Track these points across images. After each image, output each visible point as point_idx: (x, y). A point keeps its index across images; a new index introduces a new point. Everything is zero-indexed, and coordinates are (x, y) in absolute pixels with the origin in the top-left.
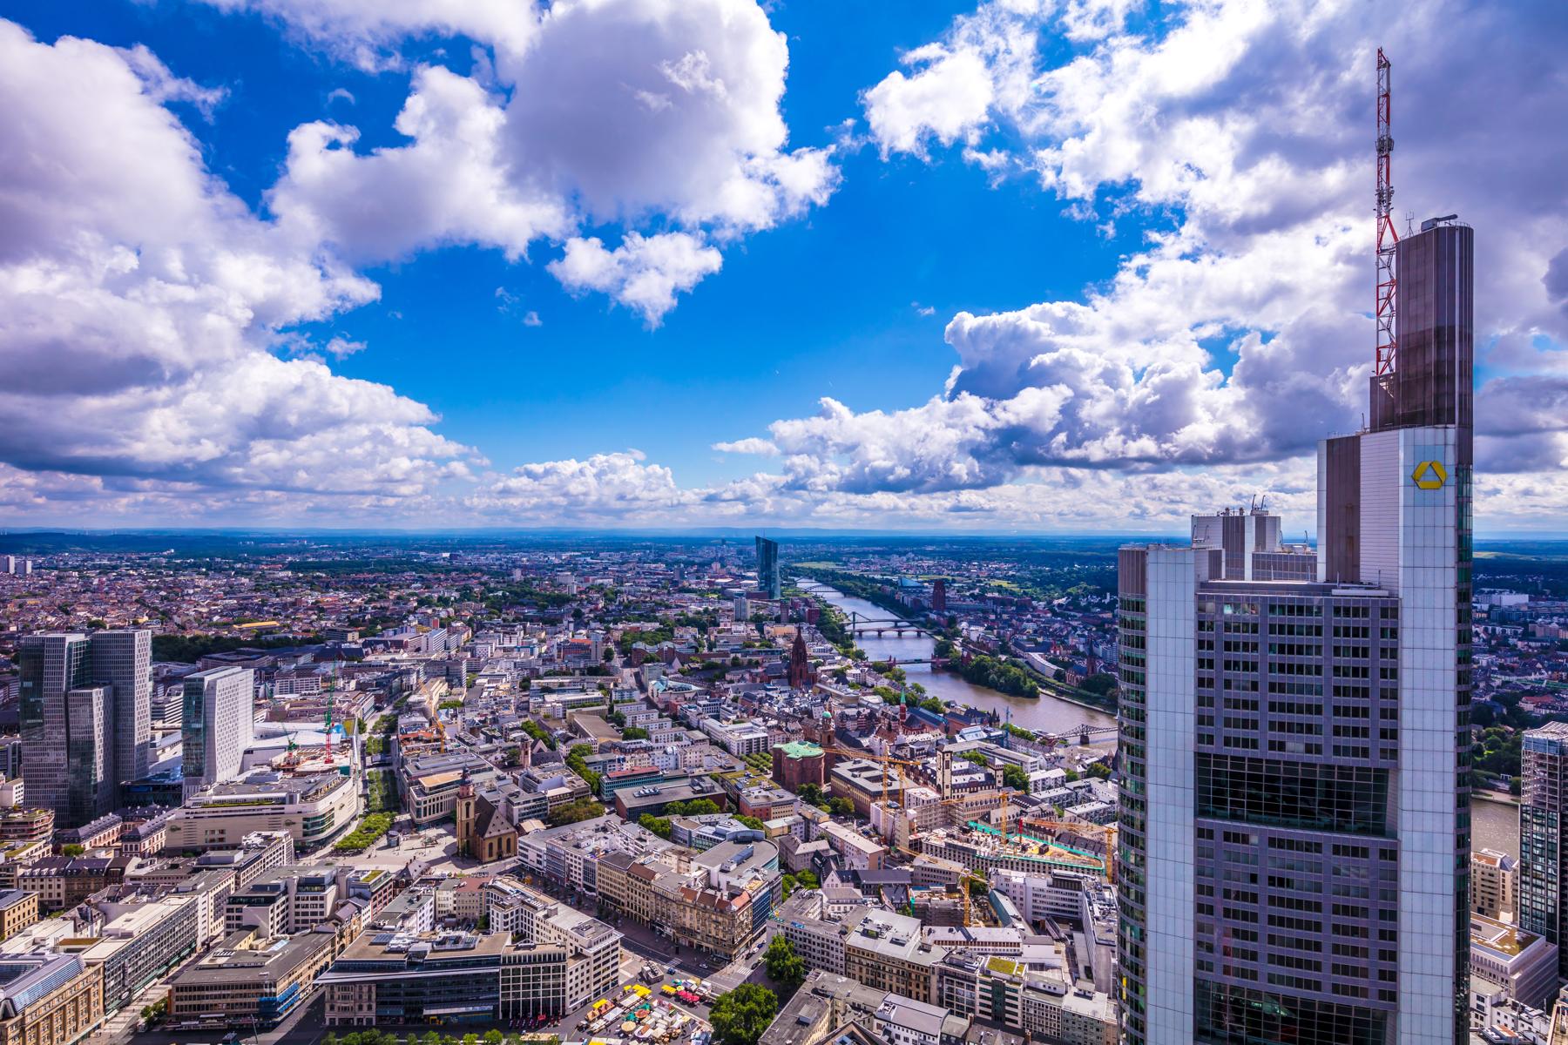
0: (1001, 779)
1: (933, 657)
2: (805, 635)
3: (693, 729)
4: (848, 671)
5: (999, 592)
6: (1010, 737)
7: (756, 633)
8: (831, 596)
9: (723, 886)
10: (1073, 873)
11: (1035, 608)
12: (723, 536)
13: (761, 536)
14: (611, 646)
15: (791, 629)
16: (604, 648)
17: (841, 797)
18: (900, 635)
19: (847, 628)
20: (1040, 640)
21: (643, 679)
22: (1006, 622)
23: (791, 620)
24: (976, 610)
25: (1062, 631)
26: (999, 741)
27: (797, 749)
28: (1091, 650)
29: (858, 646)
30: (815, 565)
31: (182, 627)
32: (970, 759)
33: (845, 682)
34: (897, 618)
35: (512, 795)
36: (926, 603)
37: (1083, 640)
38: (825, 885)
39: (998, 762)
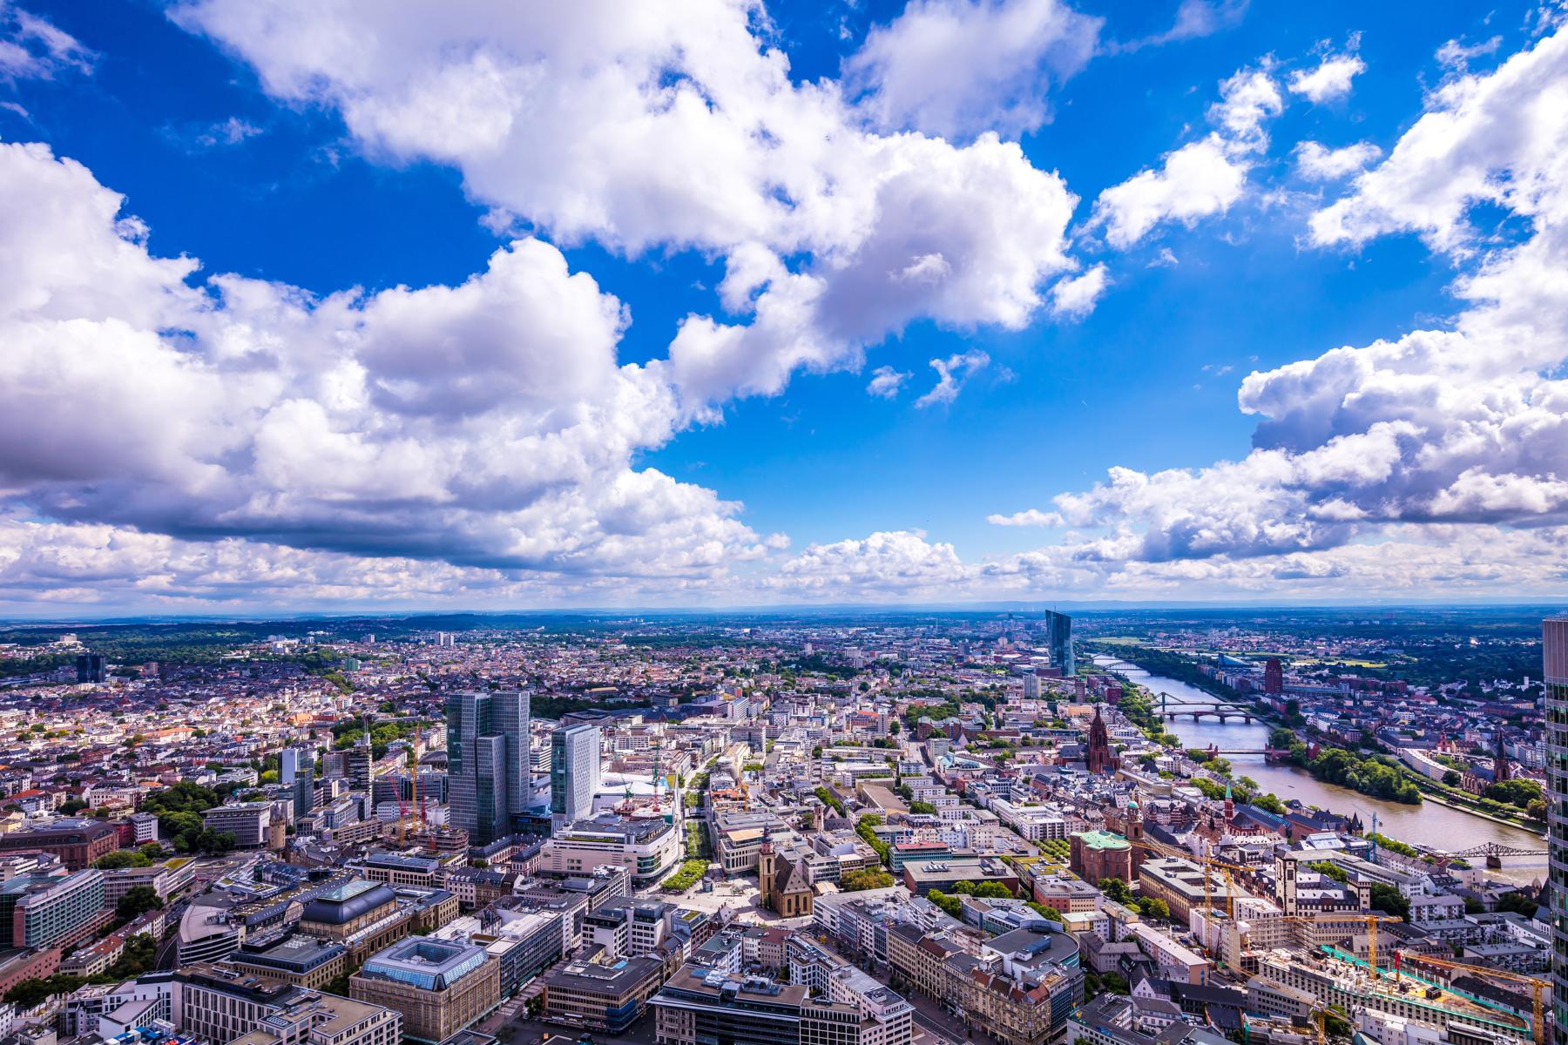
0: (1368, 899)
1: (1268, 747)
2: (1104, 716)
3: (981, 808)
4: (1158, 758)
5: (1358, 673)
6: (1379, 850)
7: (1049, 712)
8: (1135, 675)
9: (1018, 975)
10: (1480, 1030)
11: (1411, 694)
12: (1010, 610)
13: (1052, 609)
14: (897, 719)
15: (1088, 709)
16: (890, 721)
17: (1153, 897)
18: (1222, 722)
19: (1155, 710)
20: (1421, 733)
21: (929, 754)
22: (1368, 709)
23: (1087, 700)
24: (1326, 695)
25: (1453, 722)
26: (1364, 853)
27: (1098, 840)
28: (1500, 749)
29: (1169, 730)
30: (1114, 641)
31: (550, 690)
32: (1322, 871)
33: (1155, 770)
34: (1217, 701)
35: (807, 856)
36: (1256, 685)
37: (1487, 735)
38: (1135, 993)
39: (1361, 878)
